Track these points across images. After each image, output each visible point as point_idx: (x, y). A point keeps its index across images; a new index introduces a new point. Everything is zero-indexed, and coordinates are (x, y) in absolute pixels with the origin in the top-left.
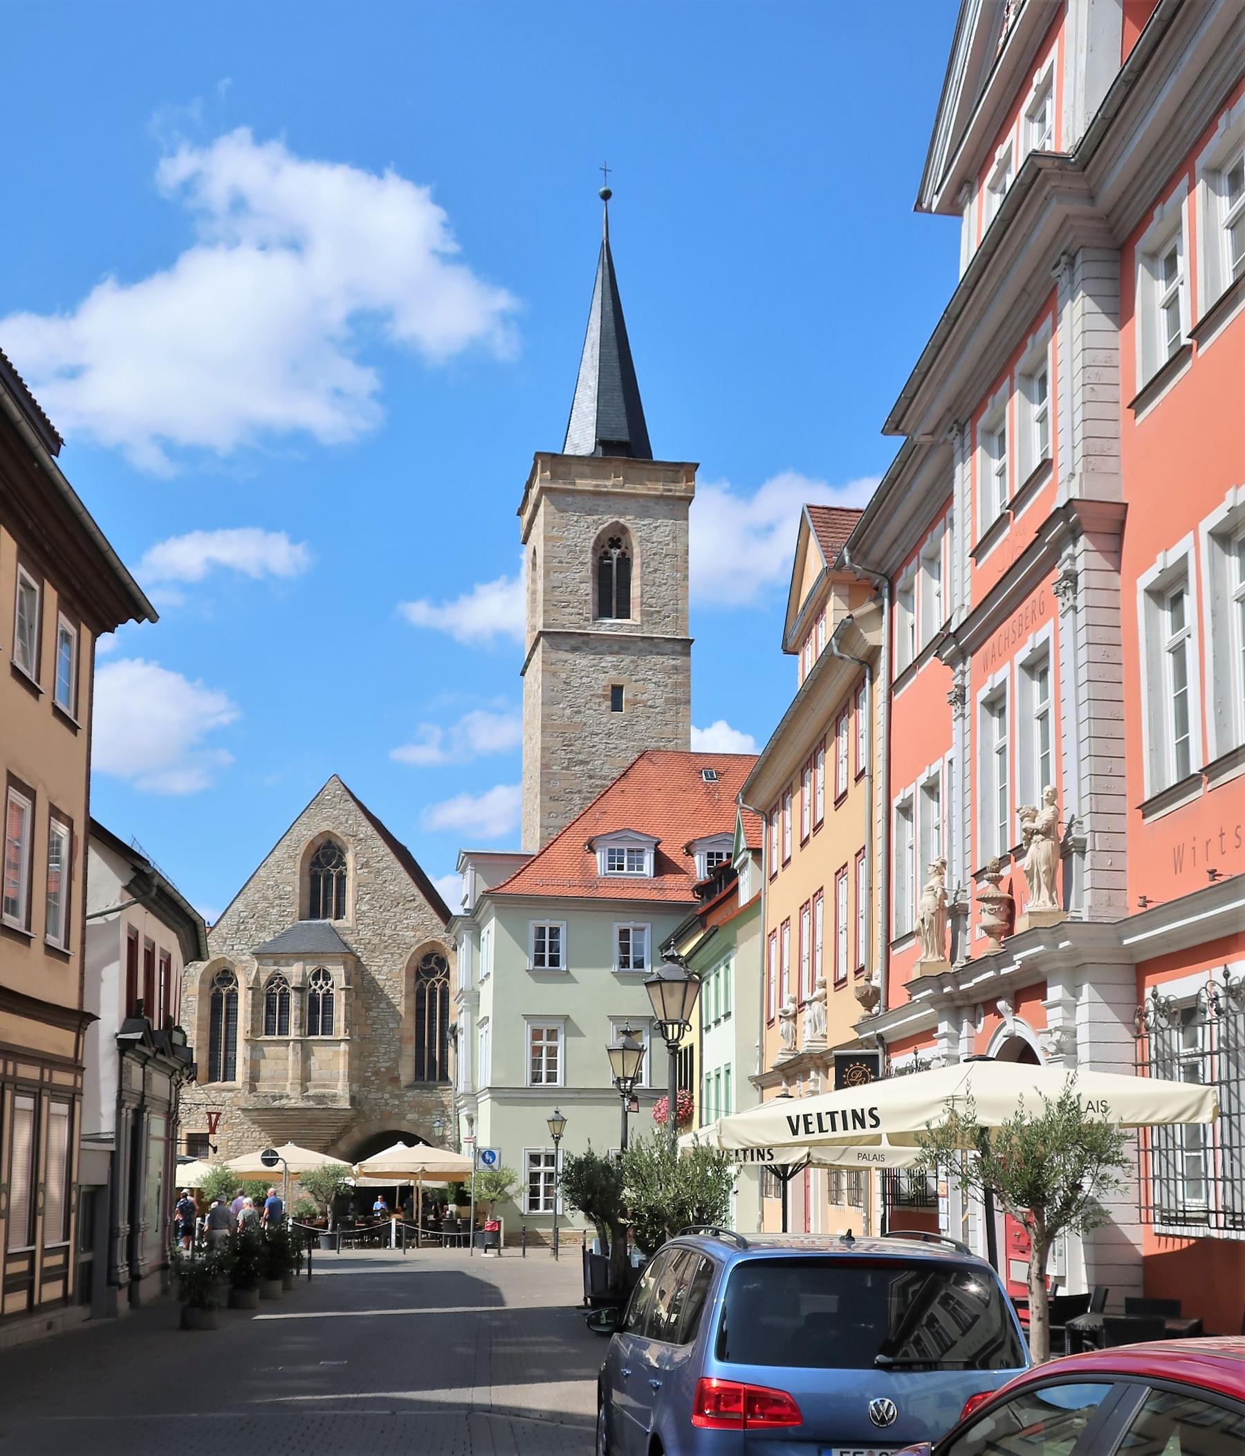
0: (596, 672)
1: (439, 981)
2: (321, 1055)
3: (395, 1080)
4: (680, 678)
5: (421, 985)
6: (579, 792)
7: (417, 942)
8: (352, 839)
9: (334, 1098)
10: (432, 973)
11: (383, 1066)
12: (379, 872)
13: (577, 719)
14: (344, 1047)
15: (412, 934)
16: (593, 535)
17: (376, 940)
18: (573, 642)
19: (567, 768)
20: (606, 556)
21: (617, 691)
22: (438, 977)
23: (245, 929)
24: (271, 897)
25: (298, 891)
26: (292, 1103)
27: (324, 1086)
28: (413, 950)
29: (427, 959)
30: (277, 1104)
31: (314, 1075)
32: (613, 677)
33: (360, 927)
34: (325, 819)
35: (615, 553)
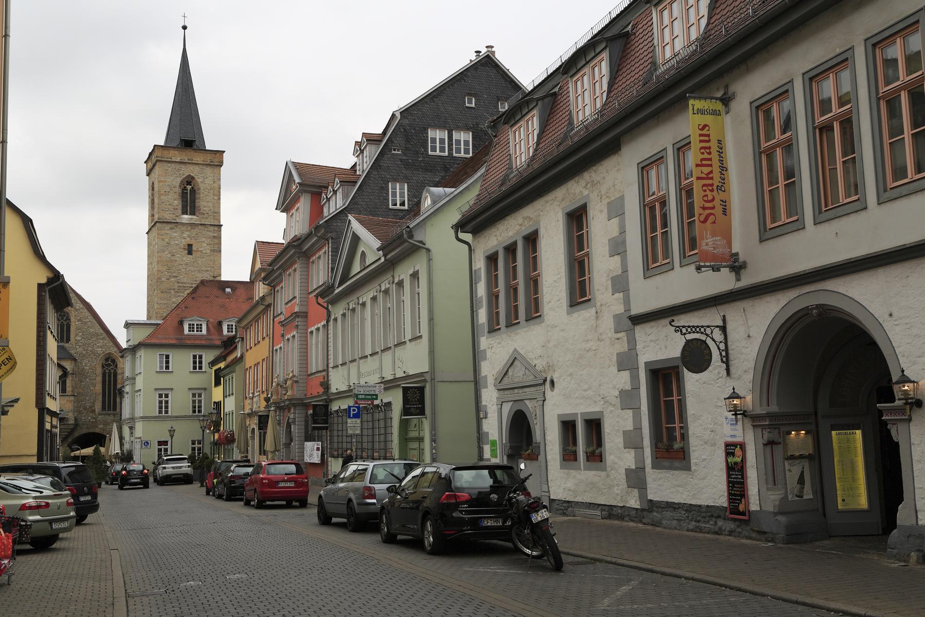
0: (181, 238)
3: (94, 411)
4: (216, 241)
11: (88, 405)
13: (173, 258)
16: (179, 180)
17: (84, 352)
18: (170, 226)
20: (185, 189)
21: (190, 246)
29: (107, 360)
32: (188, 241)
35: (189, 187)
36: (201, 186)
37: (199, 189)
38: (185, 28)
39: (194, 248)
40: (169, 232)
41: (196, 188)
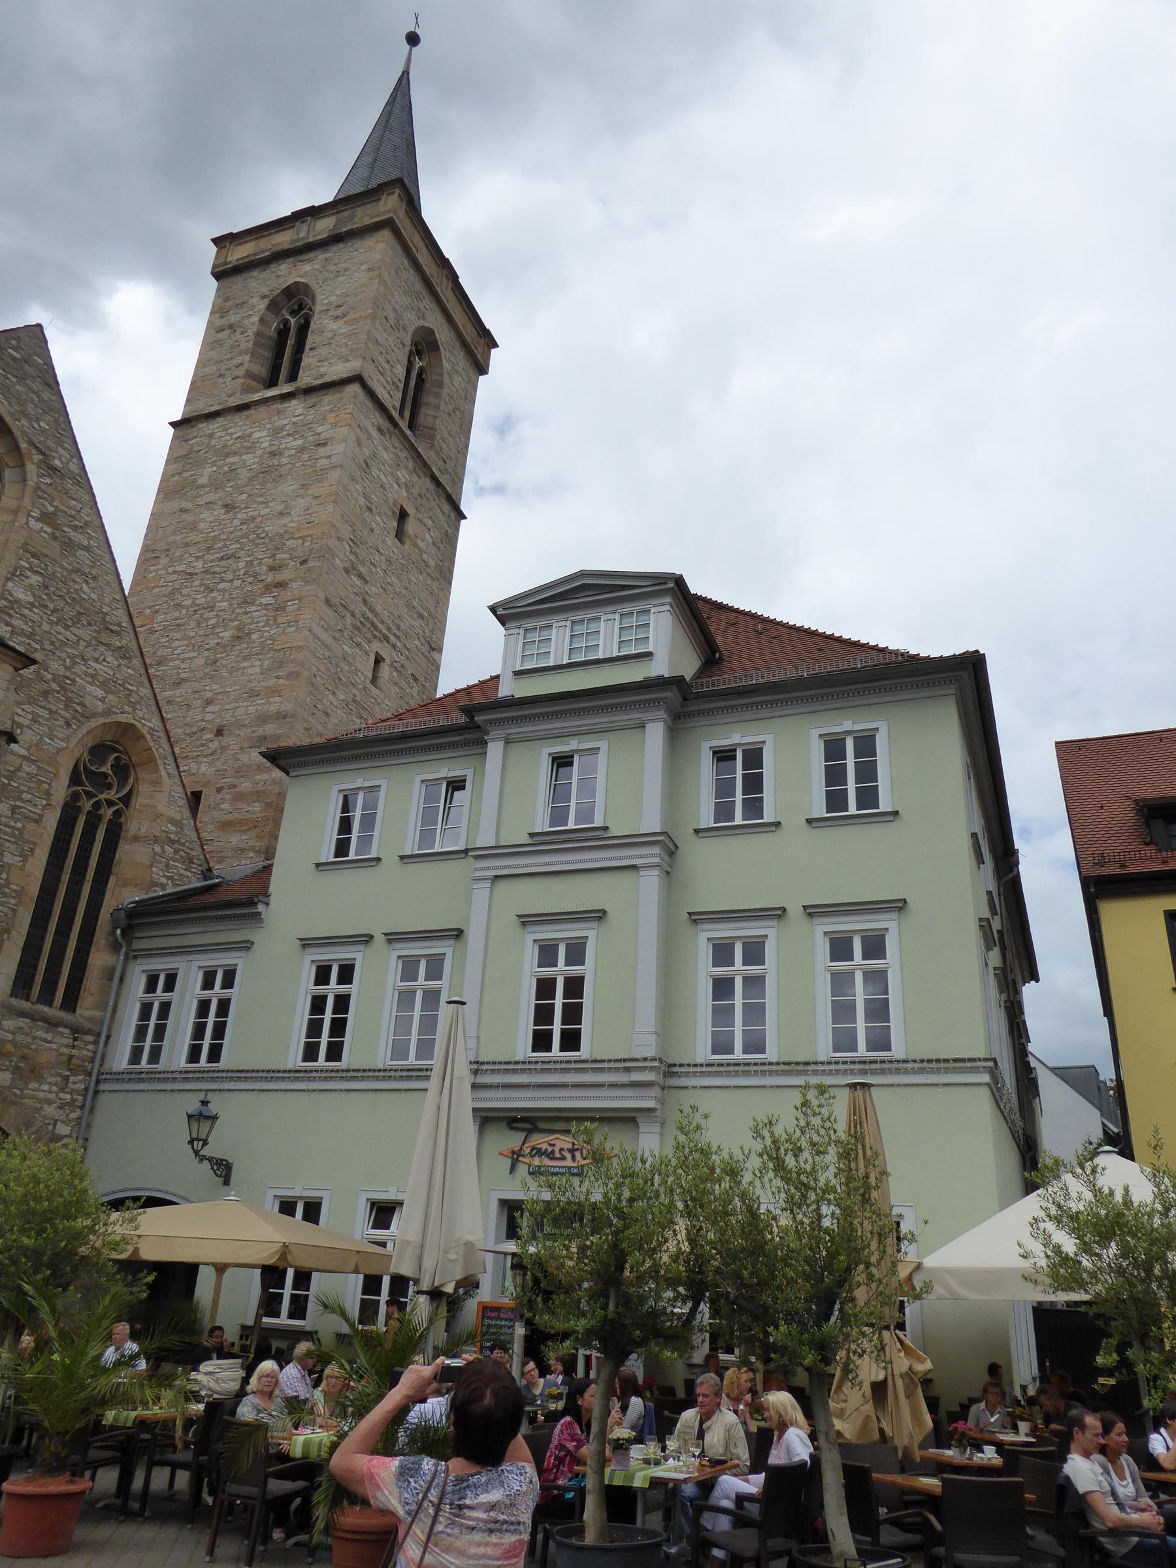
1: (110, 803)
5: (75, 796)
6: (353, 615)
7: (107, 713)
8: (37, 457)
10: (101, 781)
15: (100, 693)
19: (347, 571)
22: (112, 795)
28: (93, 723)
29: (99, 751)
36: (446, 380)
37: (441, 385)
38: (413, 39)
39: (411, 527)
40: (375, 434)
41: (430, 377)
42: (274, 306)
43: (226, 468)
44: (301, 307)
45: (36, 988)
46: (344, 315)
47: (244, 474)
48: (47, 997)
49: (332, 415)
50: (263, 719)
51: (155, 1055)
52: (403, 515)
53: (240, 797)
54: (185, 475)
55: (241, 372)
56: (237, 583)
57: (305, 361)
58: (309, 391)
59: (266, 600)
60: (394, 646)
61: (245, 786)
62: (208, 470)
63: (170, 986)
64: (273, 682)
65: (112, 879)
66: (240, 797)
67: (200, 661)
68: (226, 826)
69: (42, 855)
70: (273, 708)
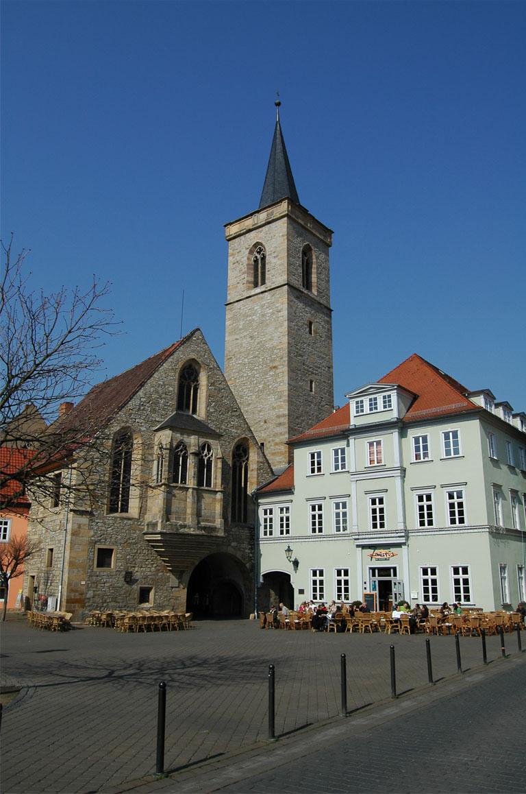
2: (207, 498)
7: (238, 436)
9: (214, 529)
12: (220, 390)
14: (219, 496)
23: (143, 410)
24: (161, 392)
25: (176, 391)
26: (191, 531)
27: (207, 521)
28: (236, 440)
30: (182, 530)
31: (203, 513)
33: (210, 421)
34: (193, 351)
42: (251, 252)
43: (248, 322)
44: (261, 250)
45: (237, 519)
46: (277, 256)
47: (255, 324)
48: (239, 520)
49: (280, 299)
50: (279, 417)
51: (271, 533)
52: (311, 323)
53: (276, 444)
54: (234, 325)
55: (245, 281)
56: (260, 367)
57: (267, 276)
58: (270, 290)
59: (271, 373)
60: (316, 374)
61: (277, 440)
62: (242, 323)
63: (271, 513)
64: (279, 403)
65: (248, 483)
66: (276, 444)
67: (254, 397)
68: (273, 454)
69: (231, 482)
70: (281, 413)
